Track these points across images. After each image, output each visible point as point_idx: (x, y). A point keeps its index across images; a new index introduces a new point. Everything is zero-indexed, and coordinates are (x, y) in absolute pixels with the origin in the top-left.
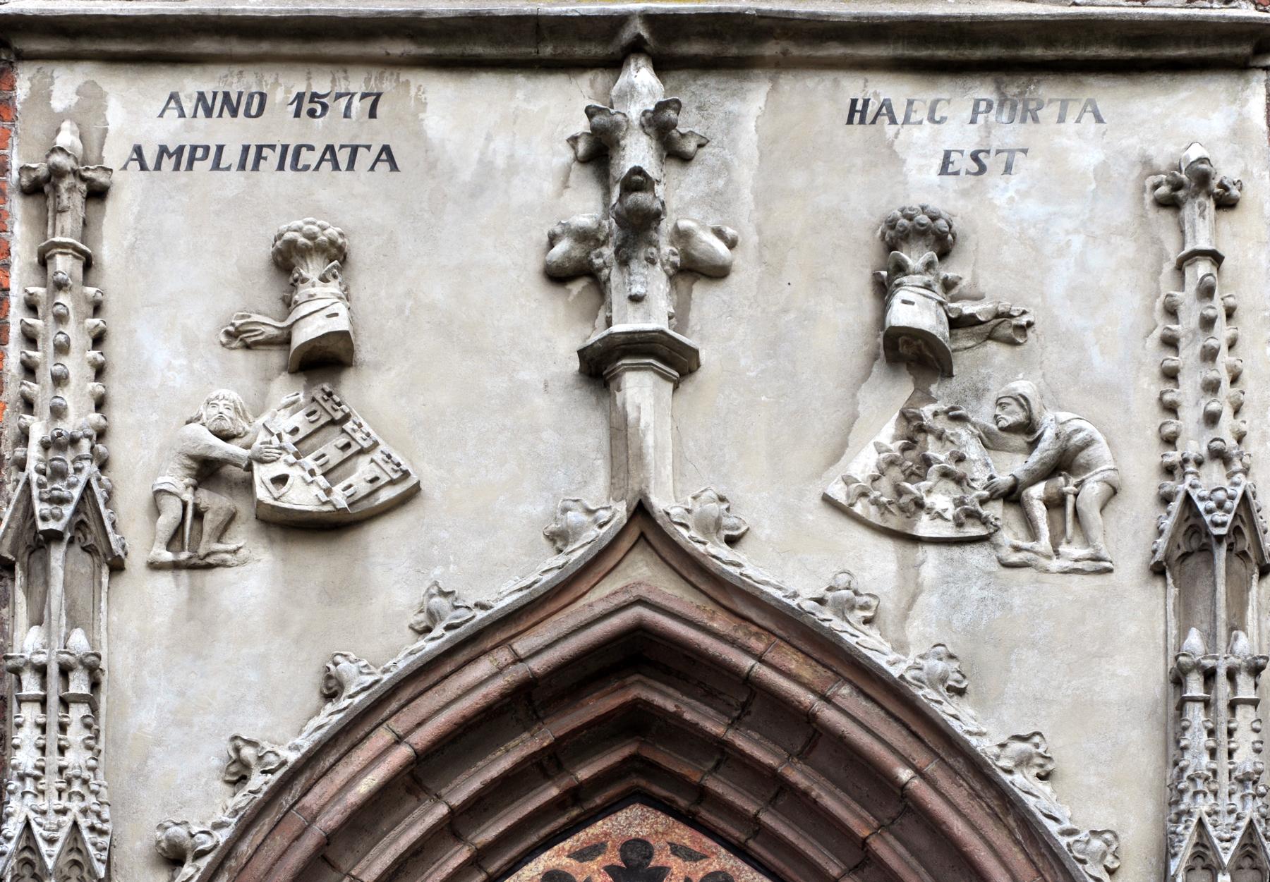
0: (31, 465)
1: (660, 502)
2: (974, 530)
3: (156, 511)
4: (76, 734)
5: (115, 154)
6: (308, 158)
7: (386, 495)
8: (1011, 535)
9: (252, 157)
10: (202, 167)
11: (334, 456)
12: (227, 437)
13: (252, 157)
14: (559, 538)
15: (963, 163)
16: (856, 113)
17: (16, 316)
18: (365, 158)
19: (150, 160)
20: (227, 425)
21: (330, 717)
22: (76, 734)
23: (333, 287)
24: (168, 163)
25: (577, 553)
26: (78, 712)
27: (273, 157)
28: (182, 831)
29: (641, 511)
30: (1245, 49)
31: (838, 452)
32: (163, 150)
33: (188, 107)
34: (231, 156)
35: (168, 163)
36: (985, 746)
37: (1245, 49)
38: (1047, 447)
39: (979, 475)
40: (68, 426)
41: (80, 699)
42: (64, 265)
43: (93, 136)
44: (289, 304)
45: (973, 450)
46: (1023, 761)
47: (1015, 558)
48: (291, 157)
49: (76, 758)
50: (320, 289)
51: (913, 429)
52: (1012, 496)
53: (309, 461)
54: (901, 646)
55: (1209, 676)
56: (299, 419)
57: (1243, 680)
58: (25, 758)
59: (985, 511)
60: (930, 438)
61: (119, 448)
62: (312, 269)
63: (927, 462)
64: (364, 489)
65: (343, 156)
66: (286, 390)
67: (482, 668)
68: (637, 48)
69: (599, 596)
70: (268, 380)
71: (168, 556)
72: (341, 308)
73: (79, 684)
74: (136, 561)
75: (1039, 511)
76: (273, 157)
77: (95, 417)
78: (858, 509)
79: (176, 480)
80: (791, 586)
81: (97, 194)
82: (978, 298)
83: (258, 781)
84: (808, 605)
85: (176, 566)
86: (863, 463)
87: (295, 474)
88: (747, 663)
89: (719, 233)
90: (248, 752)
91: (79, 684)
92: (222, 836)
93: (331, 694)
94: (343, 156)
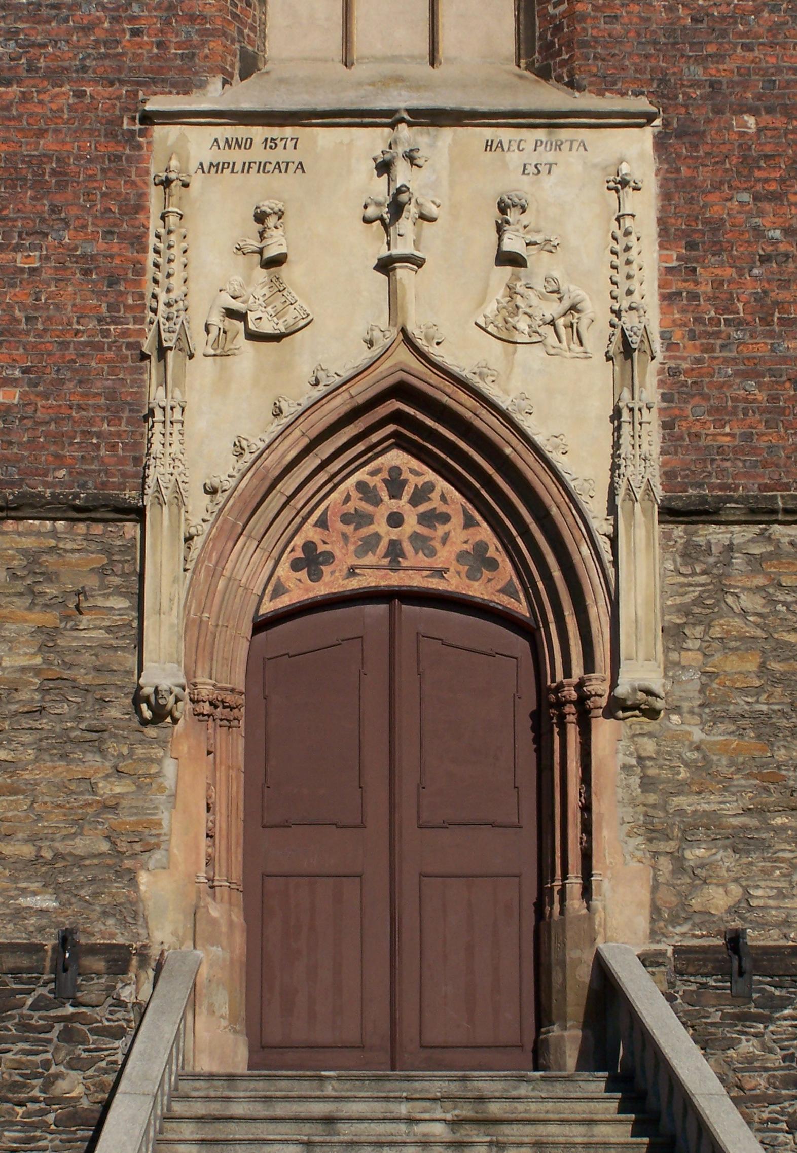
0: (160, 313)
1: (410, 328)
2: (536, 338)
3: (208, 330)
4: (176, 437)
5: (193, 166)
6: (269, 168)
7: (302, 323)
8: (552, 339)
9: (247, 167)
10: (227, 172)
11: (280, 307)
12: (234, 298)
13: (247, 167)
14: (370, 343)
15: (531, 169)
16: (489, 146)
17: (152, 241)
18: (292, 167)
19: (206, 169)
20: (237, 294)
21: (276, 427)
22: (176, 437)
23: (280, 231)
24: (213, 170)
25: (377, 350)
26: (177, 426)
27: (255, 167)
28: (217, 480)
29: (403, 331)
30: (644, 121)
31: (481, 302)
32: (211, 164)
33: (221, 145)
34: (238, 167)
35: (213, 170)
36: (539, 440)
37: (644, 121)
38: (566, 304)
39: (538, 314)
40: (173, 296)
41: (178, 421)
42: (172, 220)
43: (184, 160)
44: (262, 235)
45: (535, 301)
46: (556, 447)
47: (552, 351)
48: (262, 167)
49: (176, 448)
50: (275, 233)
51: (512, 292)
52: (552, 323)
53: (269, 309)
54: (506, 392)
55: (631, 410)
56: (265, 290)
57: (645, 411)
58: (156, 448)
59: (540, 330)
60: (519, 296)
61: (192, 301)
62: (271, 221)
63: (517, 307)
64: (291, 321)
65: (283, 167)
66: (261, 274)
67: (338, 401)
68: (402, 120)
69: (385, 366)
70: (252, 269)
71: (212, 352)
72: (284, 241)
73: (177, 415)
74: (198, 354)
75: (562, 331)
76: (255, 167)
77: (184, 288)
78: (489, 329)
79: (216, 319)
80: (462, 365)
81: (186, 185)
82: (539, 232)
83: (248, 458)
84: (470, 376)
85: (215, 355)
86: (491, 308)
87: (264, 316)
88: (445, 399)
89: (434, 202)
90: (244, 444)
91: (177, 415)
92: (233, 482)
93: (278, 412)
94: (283, 167)
